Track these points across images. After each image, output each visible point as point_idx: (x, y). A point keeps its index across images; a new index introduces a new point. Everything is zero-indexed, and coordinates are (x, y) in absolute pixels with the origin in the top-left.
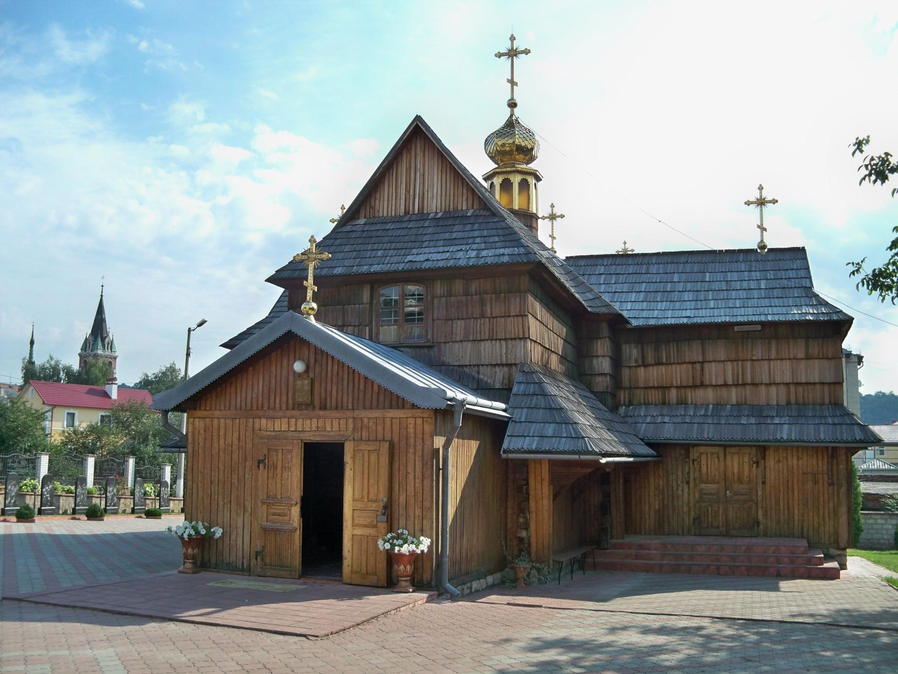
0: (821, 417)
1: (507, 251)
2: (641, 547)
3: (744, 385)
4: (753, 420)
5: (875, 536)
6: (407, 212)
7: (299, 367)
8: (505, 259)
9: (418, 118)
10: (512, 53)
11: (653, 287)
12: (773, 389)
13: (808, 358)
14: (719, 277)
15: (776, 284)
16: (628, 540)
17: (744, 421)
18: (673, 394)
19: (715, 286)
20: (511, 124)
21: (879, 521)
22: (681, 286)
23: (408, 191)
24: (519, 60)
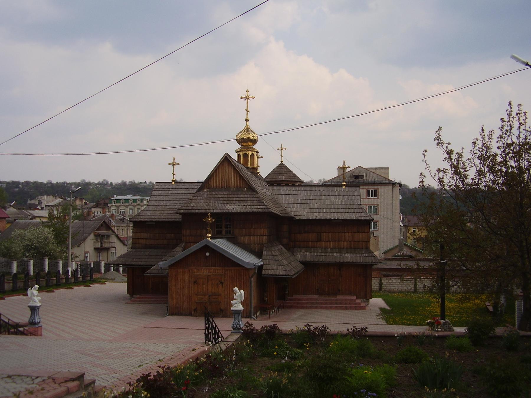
0: (362, 253)
1: (260, 207)
2: (299, 300)
3: (335, 241)
4: (338, 255)
5: (392, 288)
6: (222, 187)
7: (208, 254)
8: (260, 210)
9: (227, 154)
10: (247, 98)
11: (303, 201)
12: (346, 243)
13: (358, 232)
14: (327, 197)
15: (349, 202)
16: (295, 296)
17: (335, 255)
18: (310, 244)
19: (326, 202)
20: (247, 130)
21: (394, 281)
22: (313, 202)
23: (222, 179)
24: (250, 101)
